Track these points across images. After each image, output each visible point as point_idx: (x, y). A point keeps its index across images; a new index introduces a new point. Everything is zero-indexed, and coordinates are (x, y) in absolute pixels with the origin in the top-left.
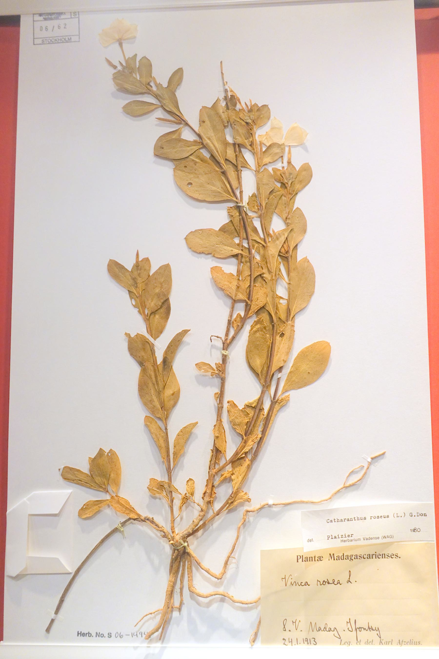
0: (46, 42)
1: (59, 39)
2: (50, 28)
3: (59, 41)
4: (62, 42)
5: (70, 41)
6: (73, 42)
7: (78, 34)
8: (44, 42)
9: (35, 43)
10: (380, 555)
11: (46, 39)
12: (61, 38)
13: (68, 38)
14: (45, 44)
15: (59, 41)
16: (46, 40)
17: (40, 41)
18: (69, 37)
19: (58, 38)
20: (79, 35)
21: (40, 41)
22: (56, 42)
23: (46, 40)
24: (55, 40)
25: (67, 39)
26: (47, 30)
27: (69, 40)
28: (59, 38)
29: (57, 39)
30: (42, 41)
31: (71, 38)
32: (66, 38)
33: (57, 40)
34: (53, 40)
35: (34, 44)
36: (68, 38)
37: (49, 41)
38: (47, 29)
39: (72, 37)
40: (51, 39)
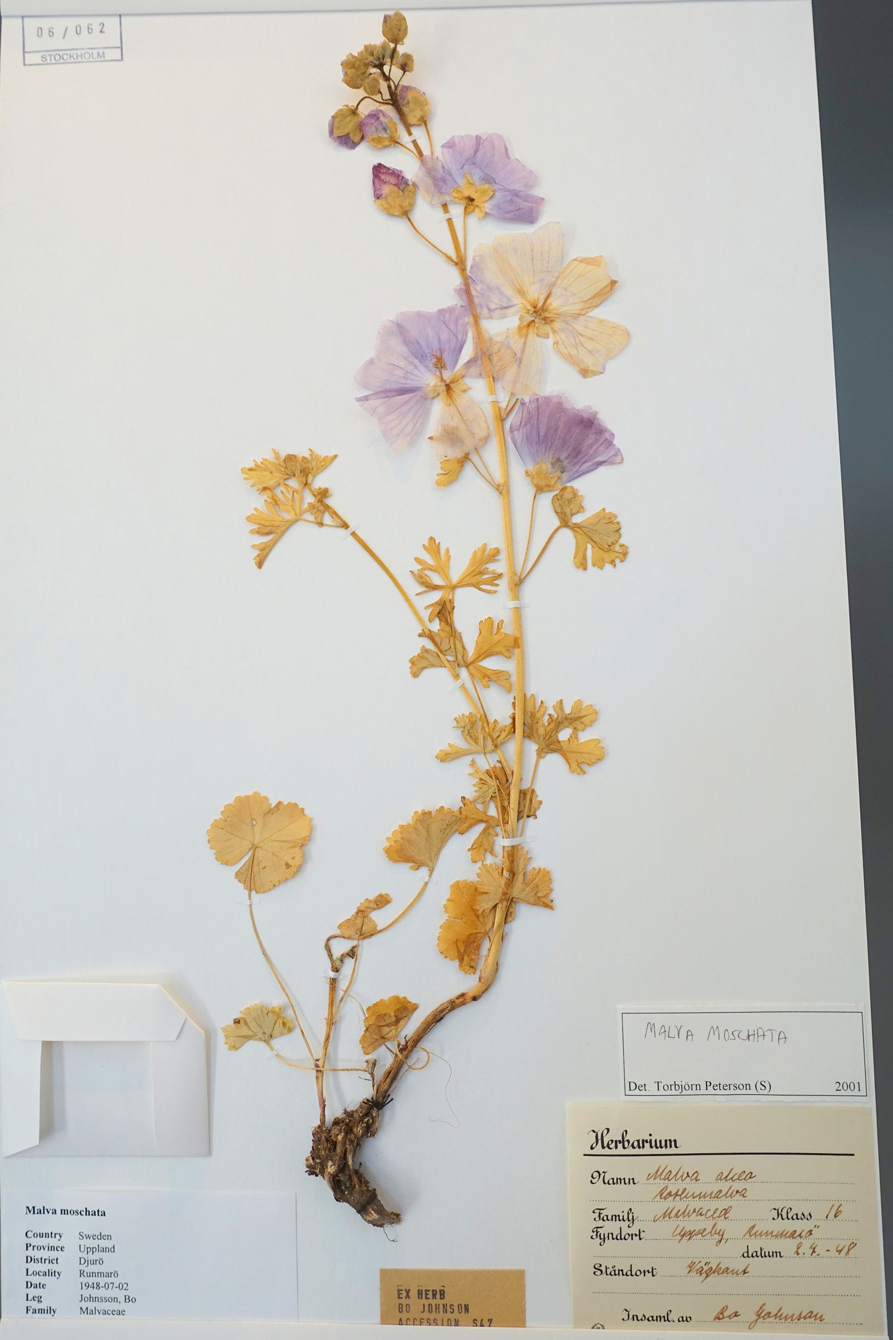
0: (51, 60)
1: (79, 54)
2: (58, 32)
4: (84, 60)
5: (103, 59)
7: (120, 45)
8: (46, 59)
9: (26, 63)
11: (50, 53)
12: (83, 52)
13: (98, 53)
14: (48, 64)
16: (51, 58)
17: (36, 58)
18: (101, 51)
22: (72, 60)
23: (50, 55)
24: (69, 59)
25: (95, 55)
26: (51, 34)
27: (101, 57)
29: (74, 54)
30: (42, 57)
31: (103, 53)
32: (92, 53)
34: (65, 57)
35: (25, 64)
36: (98, 53)
37: (57, 57)
38: (53, 33)
39: (106, 51)
40: (61, 53)
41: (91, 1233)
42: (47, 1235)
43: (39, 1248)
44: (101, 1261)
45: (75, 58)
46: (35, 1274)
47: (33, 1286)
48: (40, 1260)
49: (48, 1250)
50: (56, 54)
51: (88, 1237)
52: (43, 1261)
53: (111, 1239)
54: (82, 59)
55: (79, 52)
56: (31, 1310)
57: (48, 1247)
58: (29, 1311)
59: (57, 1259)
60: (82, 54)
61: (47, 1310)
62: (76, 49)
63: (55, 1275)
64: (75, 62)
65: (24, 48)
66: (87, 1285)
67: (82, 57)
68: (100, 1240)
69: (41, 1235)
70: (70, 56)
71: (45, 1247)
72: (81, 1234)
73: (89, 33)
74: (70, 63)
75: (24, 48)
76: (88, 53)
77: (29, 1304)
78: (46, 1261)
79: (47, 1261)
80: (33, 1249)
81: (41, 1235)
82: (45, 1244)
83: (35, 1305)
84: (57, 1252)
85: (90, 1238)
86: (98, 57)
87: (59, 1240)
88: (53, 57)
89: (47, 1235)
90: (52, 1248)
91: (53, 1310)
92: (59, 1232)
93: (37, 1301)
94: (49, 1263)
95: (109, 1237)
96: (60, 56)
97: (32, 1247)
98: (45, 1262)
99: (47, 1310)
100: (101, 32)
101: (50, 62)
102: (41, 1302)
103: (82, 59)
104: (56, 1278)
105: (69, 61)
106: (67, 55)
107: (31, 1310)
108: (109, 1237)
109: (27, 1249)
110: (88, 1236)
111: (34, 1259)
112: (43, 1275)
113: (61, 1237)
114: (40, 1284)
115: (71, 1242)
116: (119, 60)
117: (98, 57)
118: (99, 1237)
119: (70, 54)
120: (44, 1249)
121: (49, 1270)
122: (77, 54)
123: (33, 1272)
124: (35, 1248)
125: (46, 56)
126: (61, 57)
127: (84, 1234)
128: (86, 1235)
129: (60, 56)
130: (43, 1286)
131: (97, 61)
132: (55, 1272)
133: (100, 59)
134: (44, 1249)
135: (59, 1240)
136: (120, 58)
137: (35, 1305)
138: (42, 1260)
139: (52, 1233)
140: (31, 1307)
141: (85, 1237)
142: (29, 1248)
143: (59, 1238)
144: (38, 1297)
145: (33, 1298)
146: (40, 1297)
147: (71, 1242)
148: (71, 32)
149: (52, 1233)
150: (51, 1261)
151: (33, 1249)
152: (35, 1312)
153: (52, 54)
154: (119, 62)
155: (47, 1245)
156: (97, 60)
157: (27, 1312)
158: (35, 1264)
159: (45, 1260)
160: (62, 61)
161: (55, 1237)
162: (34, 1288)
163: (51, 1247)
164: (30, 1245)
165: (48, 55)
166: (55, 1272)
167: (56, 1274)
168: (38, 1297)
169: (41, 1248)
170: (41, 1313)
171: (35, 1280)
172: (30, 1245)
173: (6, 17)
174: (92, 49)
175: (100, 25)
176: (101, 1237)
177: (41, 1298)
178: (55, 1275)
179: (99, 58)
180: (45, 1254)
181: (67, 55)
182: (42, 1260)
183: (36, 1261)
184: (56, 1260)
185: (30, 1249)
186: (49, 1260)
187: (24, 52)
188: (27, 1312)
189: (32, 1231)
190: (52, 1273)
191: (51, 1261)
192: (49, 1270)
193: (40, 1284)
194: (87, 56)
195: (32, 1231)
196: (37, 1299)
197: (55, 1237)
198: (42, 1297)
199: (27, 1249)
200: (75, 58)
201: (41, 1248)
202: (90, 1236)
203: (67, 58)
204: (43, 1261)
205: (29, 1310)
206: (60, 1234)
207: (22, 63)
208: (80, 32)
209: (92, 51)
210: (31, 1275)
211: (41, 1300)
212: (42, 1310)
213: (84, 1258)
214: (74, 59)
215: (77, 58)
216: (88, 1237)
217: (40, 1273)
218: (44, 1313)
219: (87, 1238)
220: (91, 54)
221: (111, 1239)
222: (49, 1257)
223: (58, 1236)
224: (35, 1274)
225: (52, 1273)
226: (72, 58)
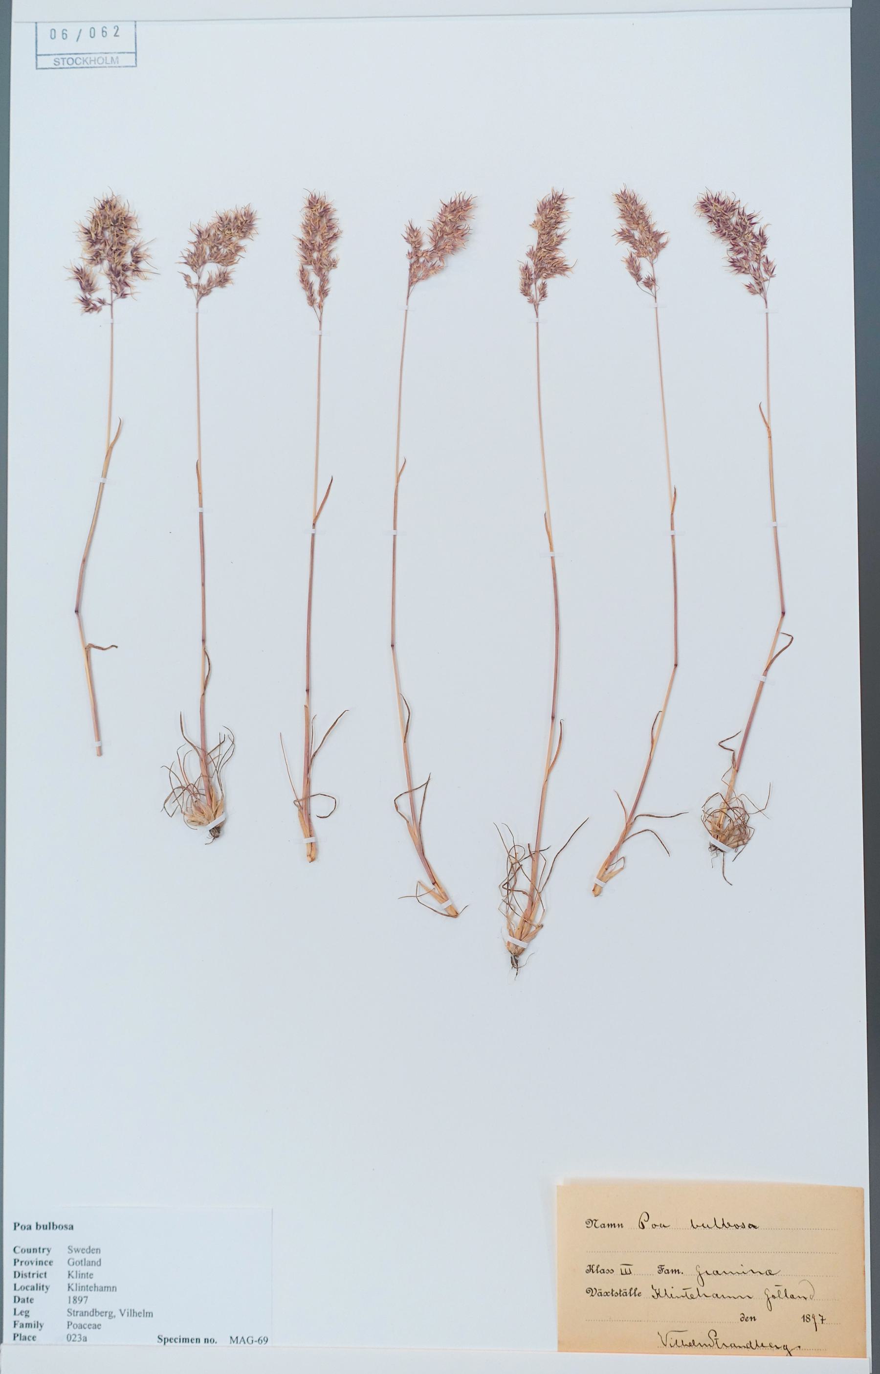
0: (63, 64)
3: (93, 62)
4: (97, 65)
5: (116, 65)
6: (119, 67)
7: (134, 51)
12: (97, 56)
15: (93, 62)
16: (63, 61)
17: (49, 62)
18: (115, 56)
20: (136, 53)
21: (49, 62)
22: (86, 65)
24: (82, 63)
25: (109, 60)
27: (115, 63)
28: (93, 57)
29: (87, 58)
30: (55, 61)
31: (117, 57)
32: (106, 58)
33: (88, 61)
34: (78, 61)
37: (70, 61)
40: (74, 57)
41: (80, 1247)
42: (35, 1250)
43: (27, 1263)
44: (90, 1276)
45: (88, 62)
47: (21, 1301)
48: (28, 1275)
49: (37, 1264)
50: (69, 58)
51: (77, 1251)
52: (31, 1275)
54: (95, 63)
55: (93, 57)
56: (19, 1323)
58: (16, 1326)
59: (45, 1273)
61: (35, 1325)
64: (88, 67)
67: (95, 61)
69: (29, 1251)
73: (104, 36)
77: (17, 1318)
79: (35, 1276)
80: (21, 1264)
81: (29, 1251)
83: (22, 1319)
84: (46, 1266)
85: (79, 1252)
86: (112, 63)
87: (47, 1255)
88: (65, 60)
89: (35, 1250)
90: (41, 1263)
91: (40, 1324)
92: (47, 1247)
93: (24, 1316)
94: (37, 1277)
95: (98, 1250)
96: (73, 60)
97: (20, 1262)
98: (33, 1277)
99: (35, 1325)
100: (115, 35)
101: (62, 66)
102: (28, 1316)
103: (95, 63)
105: (82, 65)
106: (80, 59)
107: (19, 1323)
108: (98, 1251)
109: (15, 1265)
111: (22, 1274)
112: (31, 1290)
113: (49, 1251)
114: (28, 1298)
115: (59, 1256)
118: (88, 1251)
119: (83, 58)
120: (32, 1264)
121: (37, 1285)
122: (90, 58)
123: (21, 1288)
124: (23, 1263)
125: (59, 59)
126: (74, 61)
127: (73, 1247)
128: (75, 1249)
129: (73, 60)
130: (31, 1300)
132: (43, 1286)
134: (32, 1264)
136: (135, 65)
137: (22, 1319)
138: (29, 1275)
139: (40, 1248)
140: (18, 1321)
141: (74, 1250)
142: (17, 1264)
145: (21, 1313)
146: (27, 1312)
147: (59, 1256)
148: (85, 34)
149: (40, 1248)
150: (39, 1276)
151: (21, 1264)
152: (22, 1326)
153: (65, 58)
154: (134, 68)
157: (15, 1327)
158: (23, 1279)
159: (33, 1274)
161: (43, 1252)
163: (40, 1262)
164: (18, 1261)
165: (62, 58)
166: (43, 1286)
167: (45, 1288)
168: (26, 1312)
171: (23, 1294)
172: (18, 1261)
174: (106, 53)
175: (115, 28)
176: (90, 1250)
178: (43, 1289)
180: (33, 1269)
181: (80, 59)
182: (29, 1275)
183: (24, 1276)
185: (18, 1264)
186: (38, 1274)
188: (15, 1327)
189: (20, 1247)
191: (39, 1276)
192: (37, 1285)
193: (28, 1298)
194: (100, 61)
197: (43, 1252)
198: (30, 1312)
199: (15, 1265)
200: (88, 62)
204: (31, 1275)
205: (17, 1324)
206: (48, 1249)
207: (35, 68)
211: (29, 1314)
215: (90, 63)
216: (77, 1251)
217: (28, 1288)
218: (32, 1327)
219: (76, 1252)
220: (105, 59)
223: (46, 1251)
226: (85, 63)
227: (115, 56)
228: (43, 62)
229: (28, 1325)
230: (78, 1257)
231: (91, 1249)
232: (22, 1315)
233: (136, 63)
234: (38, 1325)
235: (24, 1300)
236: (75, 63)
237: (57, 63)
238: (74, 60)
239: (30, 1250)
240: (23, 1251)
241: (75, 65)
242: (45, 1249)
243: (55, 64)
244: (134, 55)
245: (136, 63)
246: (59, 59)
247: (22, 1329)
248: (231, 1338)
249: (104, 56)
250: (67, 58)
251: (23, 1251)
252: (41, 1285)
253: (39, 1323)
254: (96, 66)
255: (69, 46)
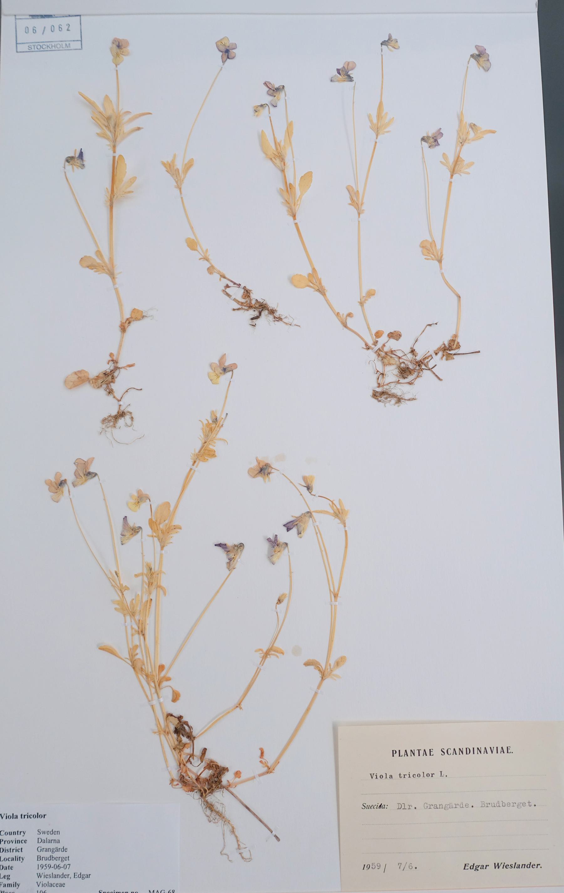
0: (34, 49)
1: (53, 45)
2: (39, 30)
4: (57, 49)
5: (69, 48)
6: (71, 50)
8: (31, 48)
10: (535, 865)
13: (66, 44)
14: (33, 51)
16: (34, 47)
17: (25, 48)
18: (67, 43)
19: (51, 43)
21: (25, 48)
22: (49, 49)
24: (46, 47)
25: (64, 46)
29: (50, 44)
30: (29, 47)
31: (69, 44)
32: (62, 44)
33: (50, 47)
34: (44, 47)
35: (17, 52)
36: (66, 44)
37: (39, 47)
38: (35, 30)
39: (71, 43)
41: (46, 830)
42: (14, 833)
43: (9, 842)
46: (5, 859)
47: (4, 868)
48: (9, 850)
49: (15, 843)
51: (44, 833)
52: (12, 850)
53: (59, 834)
56: (3, 884)
57: (16, 841)
59: (22, 849)
60: (55, 45)
62: (52, 42)
63: (20, 860)
64: (50, 51)
65: (16, 41)
66: (42, 866)
67: (55, 47)
68: (52, 835)
69: (10, 834)
70: (47, 46)
71: (13, 841)
72: (39, 830)
73: (60, 31)
74: (47, 51)
75: (16, 41)
76: (59, 44)
78: (14, 850)
79: (14, 851)
80: (5, 843)
81: (10, 834)
82: (13, 839)
85: (45, 833)
87: (23, 836)
89: (14, 833)
90: (18, 842)
91: (18, 884)
93: (6, 879)
94: (16, 851)
95: (58, 832)
96: (40, 46)
97: (3, 842)
98: (13, 852)
101: (34, 50)
103: (55, 48)
104: (20, 861)
105: (46, 49)
107: (3, 884)
108: (58, 832)
110: (44, 832)
111: (5, 850)
112: (11, 860)
113: (24, 834)
115: (32, 837)
116: (80, 49)
117: (66, 47)
118: (51, 832)
120: (12, 842)
121: (16, 857)
122: (52, 44)
123: (5, 859)
124: (6, 842)
125: (31, 46)
128: (42, 832)
129: (40, 46)
131: (65, 50)
132: (20, 858)
133: (67, 48)
134: (12, 842)
135: (23, 836)
136: (81, 48)
138: (11, 850)
139: (18, 832)
140: (2, 883)
141: (42, 833)
143: (23, 834)
144: (7, 876)
145: (4, 876)
146: (8, 876)
147: (32, 837)
149: (18, 832)
150: (17, 850)
151: (5, 843)
152: (5, 886)
153: (35, 45)
155: (15, 840)
156: (65, 49)
159: (13, 850)
160: (42, 49)
161: (20, 834)
162: (5, 869)
163: (18, 841)
164: (3, 841)
165: (33, 45)
166: (20, 858)
167: (21, 859)
168: (7, 876)
169: (10, 842)
170: (10, 886)
173: (5, 15)
174: (61, 41)
176: (53, 832)
177: (9, 876)
178: (20, 860)
179: (67, 47)
180: (13, 846)
182: (11, 850)
183: (6, 851)
184: (21, 850)
186: (16, 849)
187: (17, 43)
189: (4, 831)
190: (18, 858)
191: (17, 850)
192: (16, 857)
193: (9, 866)
195: (4, 831)
196: (6, 877)
197: (20, 834)
198: (10, 876)
201: (10, 842)
202: (45, 832)
203: (45, 48)
204: (12, 850)
206: (23, 832)
207: (15, 51)
208: (54, 30)
209: (62, 43)
210: (3, 861)
212: (10, 885)
213: (39, 851)
214: (50, 48)
215: (52, 48)
216: (44, 833)
217: (9, 859)
219: (43, 834)
221: (59, 834)
222: (16, 848)
223: (22, 833)
224: (5, 859)
225: (18, 858)
226: (49, 48)
227: (67, 43)
228: (20, 48)
229: (9, 885)
230: (44, 837)
231: (53, 832)
232: (5, 878)
233: (82, 47)
234: (16, 885)
235: (6, 867)
236: (42, 48)
237: (30, 48)
238: (41, 46)
239: (11, 832)
240: (6, 833)
241: (42, 49)
242: (22, 832)
243: (29, 49)
244: (80, 42)
245: (82, 47)
246: (31, 46)
247: (4, 888)
248: (150, 891)
249: (60, 43)
250: (37, 45)
251: (6, 833)
252: (19, 857)
253: (17, 883)
254: (56, 49)
255: (38, 37)
